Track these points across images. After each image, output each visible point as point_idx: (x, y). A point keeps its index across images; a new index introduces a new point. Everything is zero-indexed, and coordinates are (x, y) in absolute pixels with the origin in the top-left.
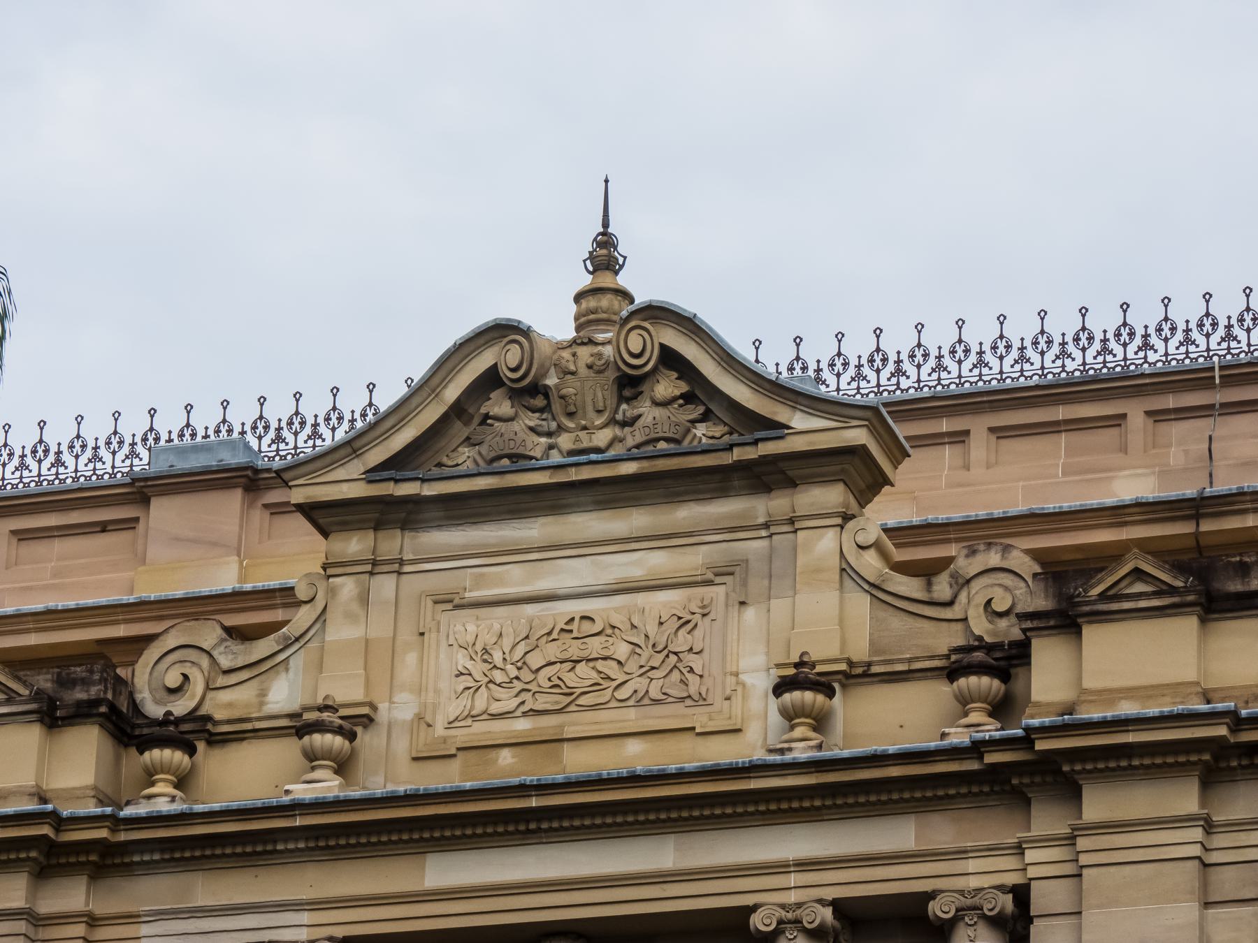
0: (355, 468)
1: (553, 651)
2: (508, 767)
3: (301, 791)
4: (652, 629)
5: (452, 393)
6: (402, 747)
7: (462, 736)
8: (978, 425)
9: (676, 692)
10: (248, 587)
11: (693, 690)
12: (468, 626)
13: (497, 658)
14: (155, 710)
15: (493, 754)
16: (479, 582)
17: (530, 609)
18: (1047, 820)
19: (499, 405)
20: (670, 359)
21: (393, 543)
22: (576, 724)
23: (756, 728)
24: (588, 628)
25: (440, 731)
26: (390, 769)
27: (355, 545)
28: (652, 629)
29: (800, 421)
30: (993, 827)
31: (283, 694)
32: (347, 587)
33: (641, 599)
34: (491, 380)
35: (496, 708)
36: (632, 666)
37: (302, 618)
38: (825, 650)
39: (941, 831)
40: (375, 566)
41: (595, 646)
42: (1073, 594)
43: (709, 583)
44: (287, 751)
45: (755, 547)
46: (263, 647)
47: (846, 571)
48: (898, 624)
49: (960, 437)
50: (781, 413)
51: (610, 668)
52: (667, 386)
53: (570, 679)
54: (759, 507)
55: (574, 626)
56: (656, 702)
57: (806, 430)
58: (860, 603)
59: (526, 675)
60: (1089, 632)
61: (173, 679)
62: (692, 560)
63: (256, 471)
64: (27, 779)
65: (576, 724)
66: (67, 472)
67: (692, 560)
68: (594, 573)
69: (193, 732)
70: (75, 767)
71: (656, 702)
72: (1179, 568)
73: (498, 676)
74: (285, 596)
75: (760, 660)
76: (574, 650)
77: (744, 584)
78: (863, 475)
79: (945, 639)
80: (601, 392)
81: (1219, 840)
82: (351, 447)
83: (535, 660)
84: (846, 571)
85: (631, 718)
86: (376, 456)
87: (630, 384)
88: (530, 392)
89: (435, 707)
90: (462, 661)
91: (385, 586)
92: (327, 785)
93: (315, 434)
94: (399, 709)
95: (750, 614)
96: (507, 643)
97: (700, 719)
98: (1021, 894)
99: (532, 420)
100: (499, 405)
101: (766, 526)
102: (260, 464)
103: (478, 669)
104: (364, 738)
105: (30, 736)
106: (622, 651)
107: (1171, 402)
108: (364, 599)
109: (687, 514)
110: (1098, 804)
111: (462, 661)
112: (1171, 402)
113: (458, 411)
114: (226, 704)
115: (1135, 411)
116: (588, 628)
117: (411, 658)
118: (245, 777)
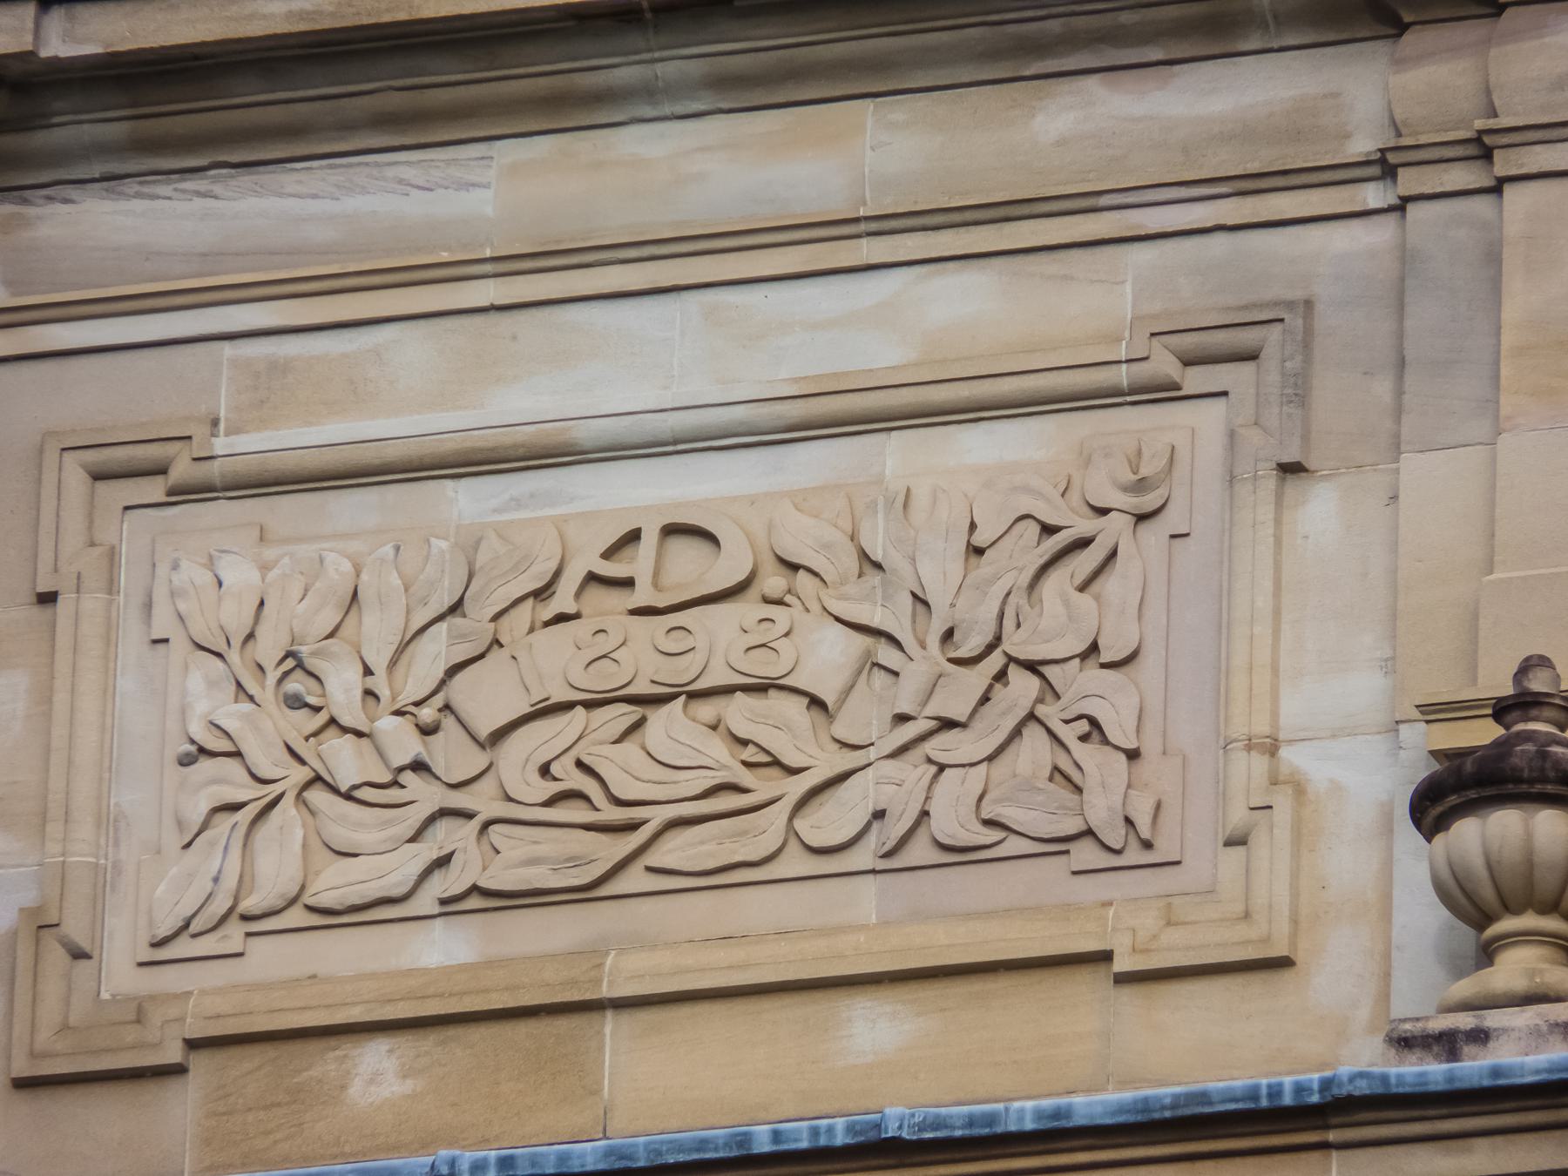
1: (556, 662)
4: (940, 571)
7: (208, 994)
9: (1041, 815)
11: (1101, 809)
12: (222, 567)
13: (341, 688)
15: (326, 1062)
16: (267, 396)
17: (469, 501)
22: (649, 941)
24: (692, 568)
25: (119, 973)
28: (940, 571)
33: (895, 455)
35: (337, 883)
36: (864, 717)
43: (1163, 392)
45: (1337, 253)
51: (779, 725)
53: (627, 769)
55: (639, 563)
56: (959, 854)
59: (453, 755)
62: (1096, 305)
65: (649, 941)
67: (1096, 305)
71: (959, 854)
73: (346, 761)
75: (1364, 690)
76: (642, 657)
77: (1299, 392)
83: (490, 697)
85: (863, 919)
89: (102, 881)
90: (204, 700)
95: (1320, 510)
96: (378, 632)
97: (1129, 921)
101: (1385, 167)
103: (265, 732)
106: (825, 656)
111: (204, 700)
116: (692, 568)
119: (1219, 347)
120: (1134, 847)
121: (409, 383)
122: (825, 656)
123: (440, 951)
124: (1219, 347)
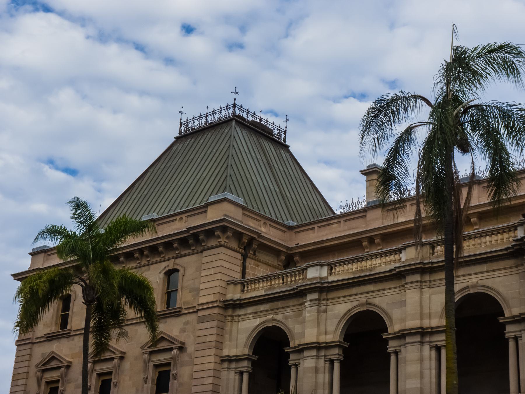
10: (480, 203)
49: (314, 228)
63: (480, 180)
66: (345, 210)
93: (361, 204)
102: (480, 179)
107: (347, 218)
112: (347, 218)
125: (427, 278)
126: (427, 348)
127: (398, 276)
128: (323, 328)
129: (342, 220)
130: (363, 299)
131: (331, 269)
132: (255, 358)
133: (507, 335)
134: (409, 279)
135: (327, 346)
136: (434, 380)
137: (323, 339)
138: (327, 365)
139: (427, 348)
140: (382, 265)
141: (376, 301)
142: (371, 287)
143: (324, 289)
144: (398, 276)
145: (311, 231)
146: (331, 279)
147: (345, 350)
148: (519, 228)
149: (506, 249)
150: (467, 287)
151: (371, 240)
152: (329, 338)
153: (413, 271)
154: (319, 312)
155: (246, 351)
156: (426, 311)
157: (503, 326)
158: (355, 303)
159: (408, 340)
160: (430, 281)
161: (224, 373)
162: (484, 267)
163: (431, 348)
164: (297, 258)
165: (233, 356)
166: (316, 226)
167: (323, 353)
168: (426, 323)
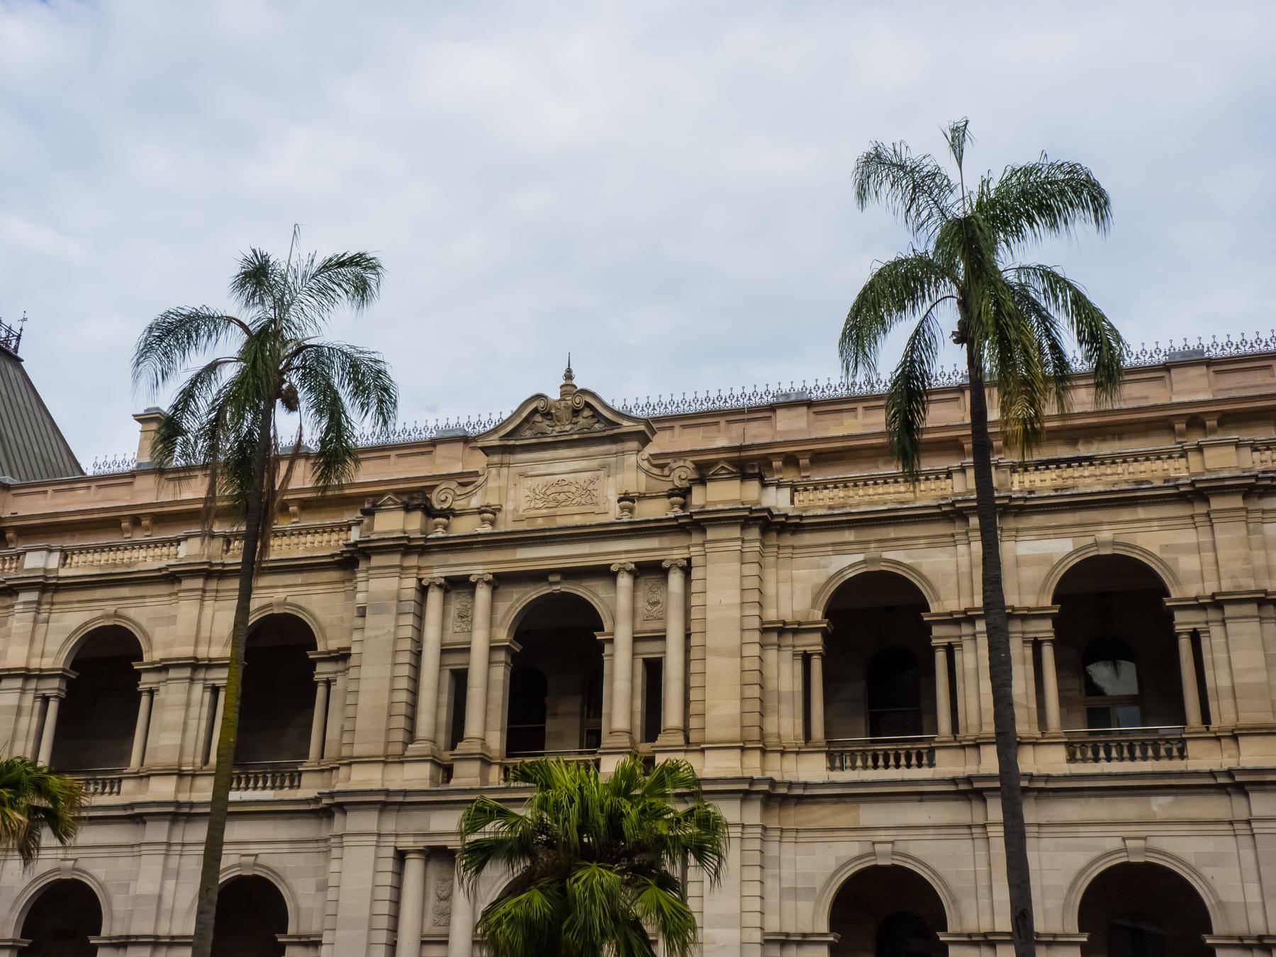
0: (496, 436)
1: (553, 490)
2: (540, 523)
3: (480, 530)
5: (524, 415)
6: (510, 517)
8: (677, 425)
12: (529, 483)
14: (438, 507)
18: (696, 538)
19: (538, 418)
20: (588, 405)
21: (507, 458)
22: (560, 511)
23: (612, 513)
26: (506, 524)
27: (496, 459)
29: (625, 423)
30: (681, 540)
31: (475, 502)
32: (494, 471)
34: (536, 411)
37: (481, 480)
38: (632, 489)
39: (666, 542)
40: (502, 465)
41: (566, 489)
42: (704, 473)
44: (477, 518)
45: (612, 460)
46: (470, 488)
47: (639, 467)
48: (654, 482)
49: (672, 428)
50: (620, 421)
52: (587, 413)
54: (613, 448)
57: (627, 426)
58: (643, 476)
60: (709, 485)
61: (443, 498)
64: (401, 527)
65: (560, 511)
66: (412, 438)
68: (565, 467)
69: (449, 513)
70: (414, 523)
72: (734, 466)
74: (476, 474)
78: (644, 439)
79: (667, 487)
80: (567, 415)
81: (746, 545)
82: (495, 430)
83: (548, 492)
84: (639, 467)
85: (576, 509)
86: (502, 433)
87: (576, 412)
88: (547, 414)
90: (527, 493)
91: (504, 470)
92: (488, 529)
94: (509, 507)
95: (611, 479)
97: (595, 509)
98: (689, 560)
99: (548, 422)
100: (538, 418)
103: (532, 495)
104: (499, 515)
105: (401, 514)
106: (574, 490)
108: (499, 475)
109: (593, 450)
110: (711, 534)
111: (527, 493)
112: (732, 418)
113: (526, 420)
114: (458, 505)
115: (722, 421)
117: (512, 492)
118: (464, 526)
119: (603, 467)
120: (597, 504)
121: (542, 469)
122: (574, 490)
123: (544, 511)
124: (603, 467)
125: (213, 585)
126: (198, 688)
127: (170, 577)
128: (38, 648)
129: (93, 485)
130: (110, 608)
131: (66, 558)
132: (517, 648)
133: (317, 678)
134: (187, 584)
135: (41, 675)
136: (202, 735)
137: (35, 663)
138: (38, 704)
139: (198, 688)
140: (148, 560)
141: (132, 613)
142: (125, 591)
143: (48, 587)
144: (170, 577)
145: (41, 497)
146: (63, 573)
147: (70, 683)
148: (353, 528)
149: (332, 556)
150: (270, 605)
151: (136, 521)
152: (47, 663)
153: (194, 574)
154: (35, 621)
155: (818, 614)
156: (205, 633)
157: (313, 663)
158: (99, 613)
159: (172, 673)
160: (779, 547)
161: (772, 655)
162: (298, 578)
163: (794, 655)
164: (10, 535)
165: (36, 670)
166: (50, 489)
167: (33, 684)
168: (202, 652)
